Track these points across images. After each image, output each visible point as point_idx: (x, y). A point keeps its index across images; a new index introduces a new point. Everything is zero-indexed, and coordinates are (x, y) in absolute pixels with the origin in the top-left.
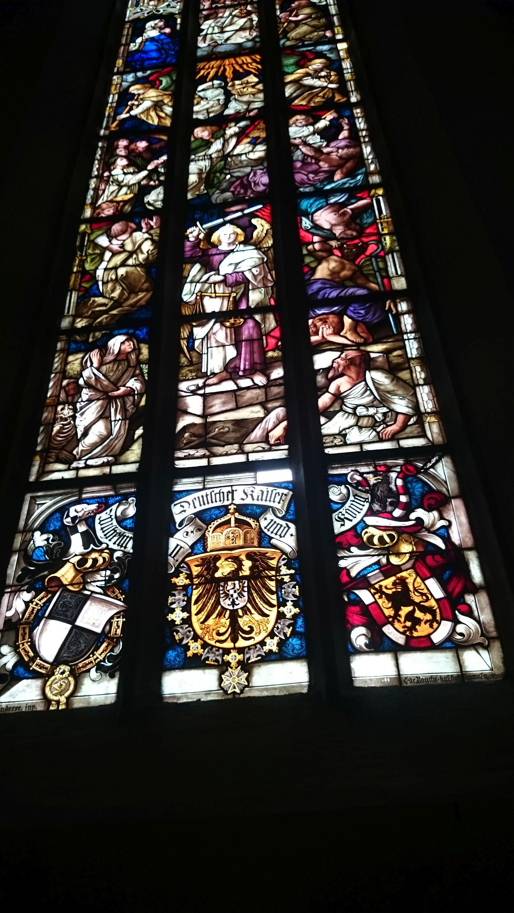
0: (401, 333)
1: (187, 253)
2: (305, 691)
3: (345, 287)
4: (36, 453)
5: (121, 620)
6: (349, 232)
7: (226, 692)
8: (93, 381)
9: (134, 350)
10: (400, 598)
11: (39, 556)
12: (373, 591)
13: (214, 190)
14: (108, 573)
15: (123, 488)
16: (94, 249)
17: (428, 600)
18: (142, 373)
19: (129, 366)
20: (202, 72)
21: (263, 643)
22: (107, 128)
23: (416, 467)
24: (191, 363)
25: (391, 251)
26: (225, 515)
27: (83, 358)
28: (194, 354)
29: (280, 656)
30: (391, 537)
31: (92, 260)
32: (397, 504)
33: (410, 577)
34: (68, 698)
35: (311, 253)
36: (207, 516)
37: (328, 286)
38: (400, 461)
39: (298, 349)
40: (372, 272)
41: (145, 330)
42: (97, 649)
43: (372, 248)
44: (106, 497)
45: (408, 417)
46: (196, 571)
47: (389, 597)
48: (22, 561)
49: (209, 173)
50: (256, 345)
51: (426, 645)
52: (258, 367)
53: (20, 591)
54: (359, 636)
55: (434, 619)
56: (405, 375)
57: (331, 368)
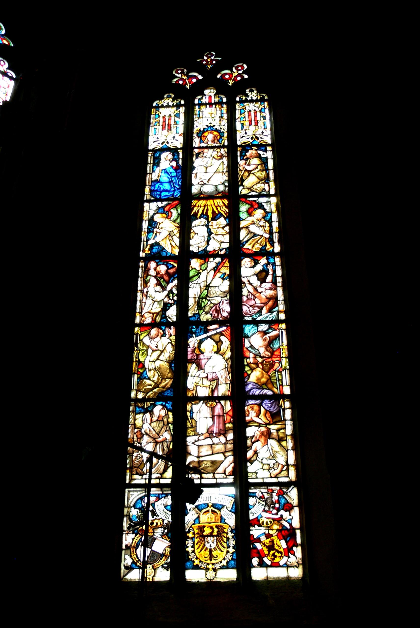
0: (285, 420)
1: (189, 356)
2: (235, 580)
3: (263, 389)
4: (127, 468)
5: (169, 549)
6: (267, 353)
7: (208, 579)
8: (148, 432)
9: (166, 415)
10: (271, 547)
11: (135, 519)
12: (262, 544)
13: (202, 311)
14: (163, 529)
15: (165, 491)
16: (143, 347)
17: (280, 548)
18: (170, 430)
19: (164, 424)
20: (195, 209)
21: (221, 562)
22: (144, 251)
23: (283, 491)
24: (192, 427)
25: (285, 369)
26: (207, 507)
27: (143, 417)
28: (193, 421)
29: (227, 567)
30: (271, 522)
31: (143, 353)
32: (274, 508)
33: (275, 538)
34: (152, 577)
35: (248, 365)
36: (200, 507)
37: (255, 387)
38: (278, 488)
39: (240, 423)
40: (275, 381)
41: (170, 404)
42: (161, 559)
43: (277, 365)
44: (159, 494)
45: (283, 466)
46: (196, 531)
47: (267, 547)
48: (128, 521)
49: (199, 298)
50: (221, 419)
51: (277, 565)
52: (222, 432)
53: (129, 533)
54: (255, 561)
55: (282, 556)
56: (284, 443)
57: (253, 436)
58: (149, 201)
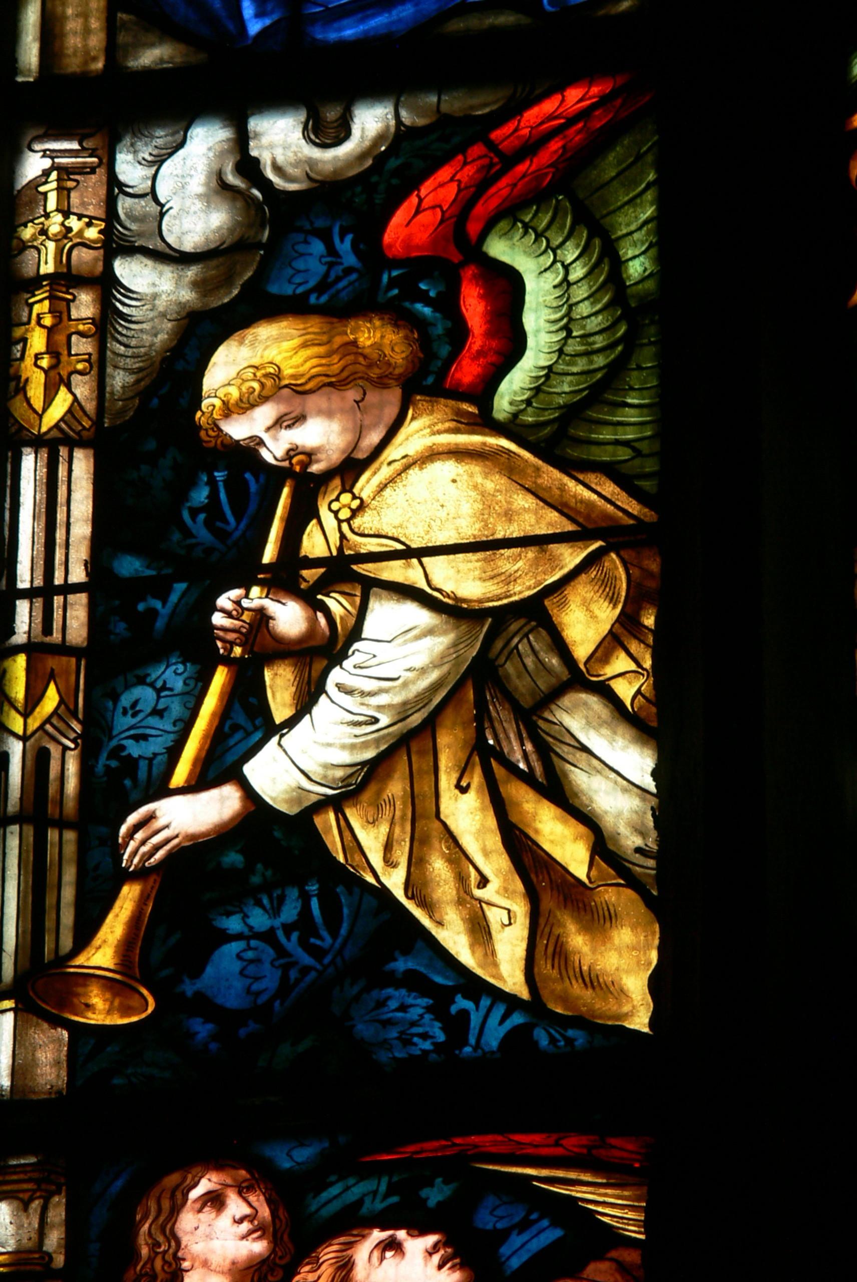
58: (113, 108)
